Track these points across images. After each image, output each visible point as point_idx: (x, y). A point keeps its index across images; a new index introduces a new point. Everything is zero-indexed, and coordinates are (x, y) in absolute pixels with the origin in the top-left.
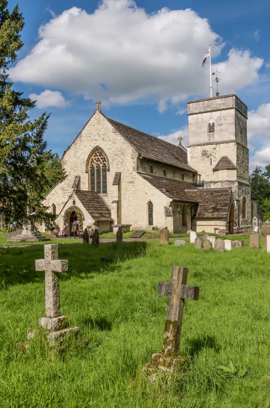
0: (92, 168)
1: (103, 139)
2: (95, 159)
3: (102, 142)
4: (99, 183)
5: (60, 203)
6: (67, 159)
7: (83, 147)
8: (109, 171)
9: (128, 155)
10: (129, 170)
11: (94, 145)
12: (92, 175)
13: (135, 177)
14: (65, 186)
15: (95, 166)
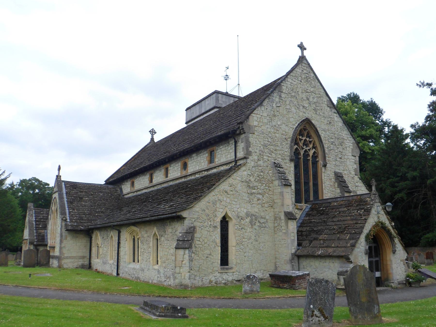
0: (296, 153)
1: (315, 110)
2: (301, 140)
3: (313, 115)
4: (307, 183)
5: (243, 214)
6: (255, 123)
7: (285, 112)
8: (325, 166)
9: (348, 148)
10: (350, 173)
11: (303, 116)
12: (297, 167)
13: (357, 184)
14: (253, 180)
15: (302, 152)
